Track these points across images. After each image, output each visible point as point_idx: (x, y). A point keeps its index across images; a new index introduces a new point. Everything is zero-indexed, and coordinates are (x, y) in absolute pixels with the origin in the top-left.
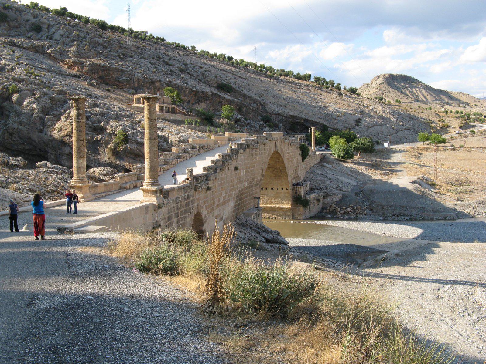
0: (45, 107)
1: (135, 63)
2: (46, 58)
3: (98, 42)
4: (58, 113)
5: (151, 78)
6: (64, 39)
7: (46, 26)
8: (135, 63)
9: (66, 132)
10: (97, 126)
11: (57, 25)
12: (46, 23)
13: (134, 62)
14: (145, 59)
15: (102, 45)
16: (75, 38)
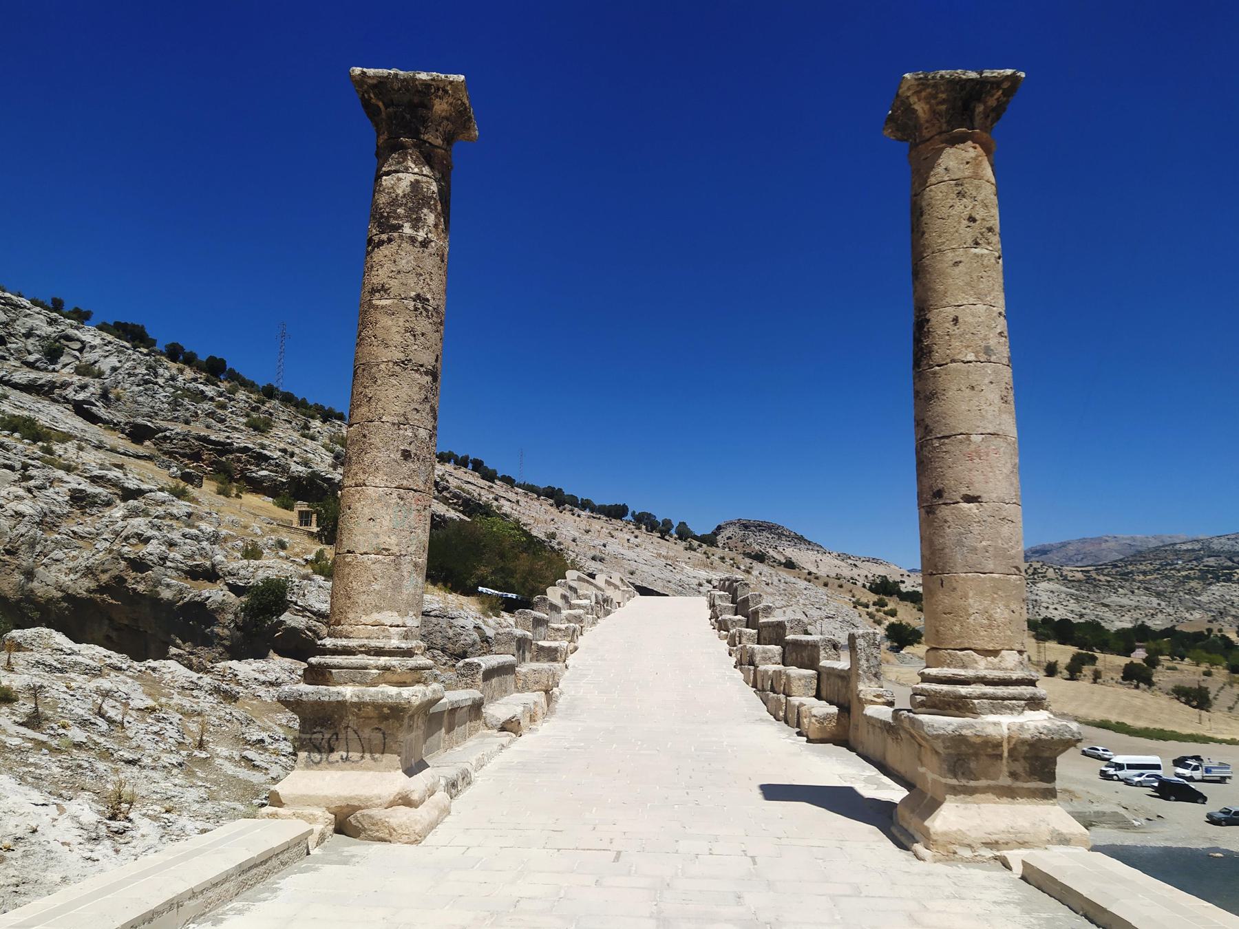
0: (52, 512)
1: (290, 444)
2: (68, 412)
3: (202, 392)
4: (88, 529)
5: (329, 476)
6: (121, 377)
7: (77, 345)
8: (290, 444)
9: (104, 578)
10: (197, 566)
11: (105, 345)
12: (78, 340)
13: (290, 441)
14: (313, 438)
15: (212, 399)
16: (147, 377)
